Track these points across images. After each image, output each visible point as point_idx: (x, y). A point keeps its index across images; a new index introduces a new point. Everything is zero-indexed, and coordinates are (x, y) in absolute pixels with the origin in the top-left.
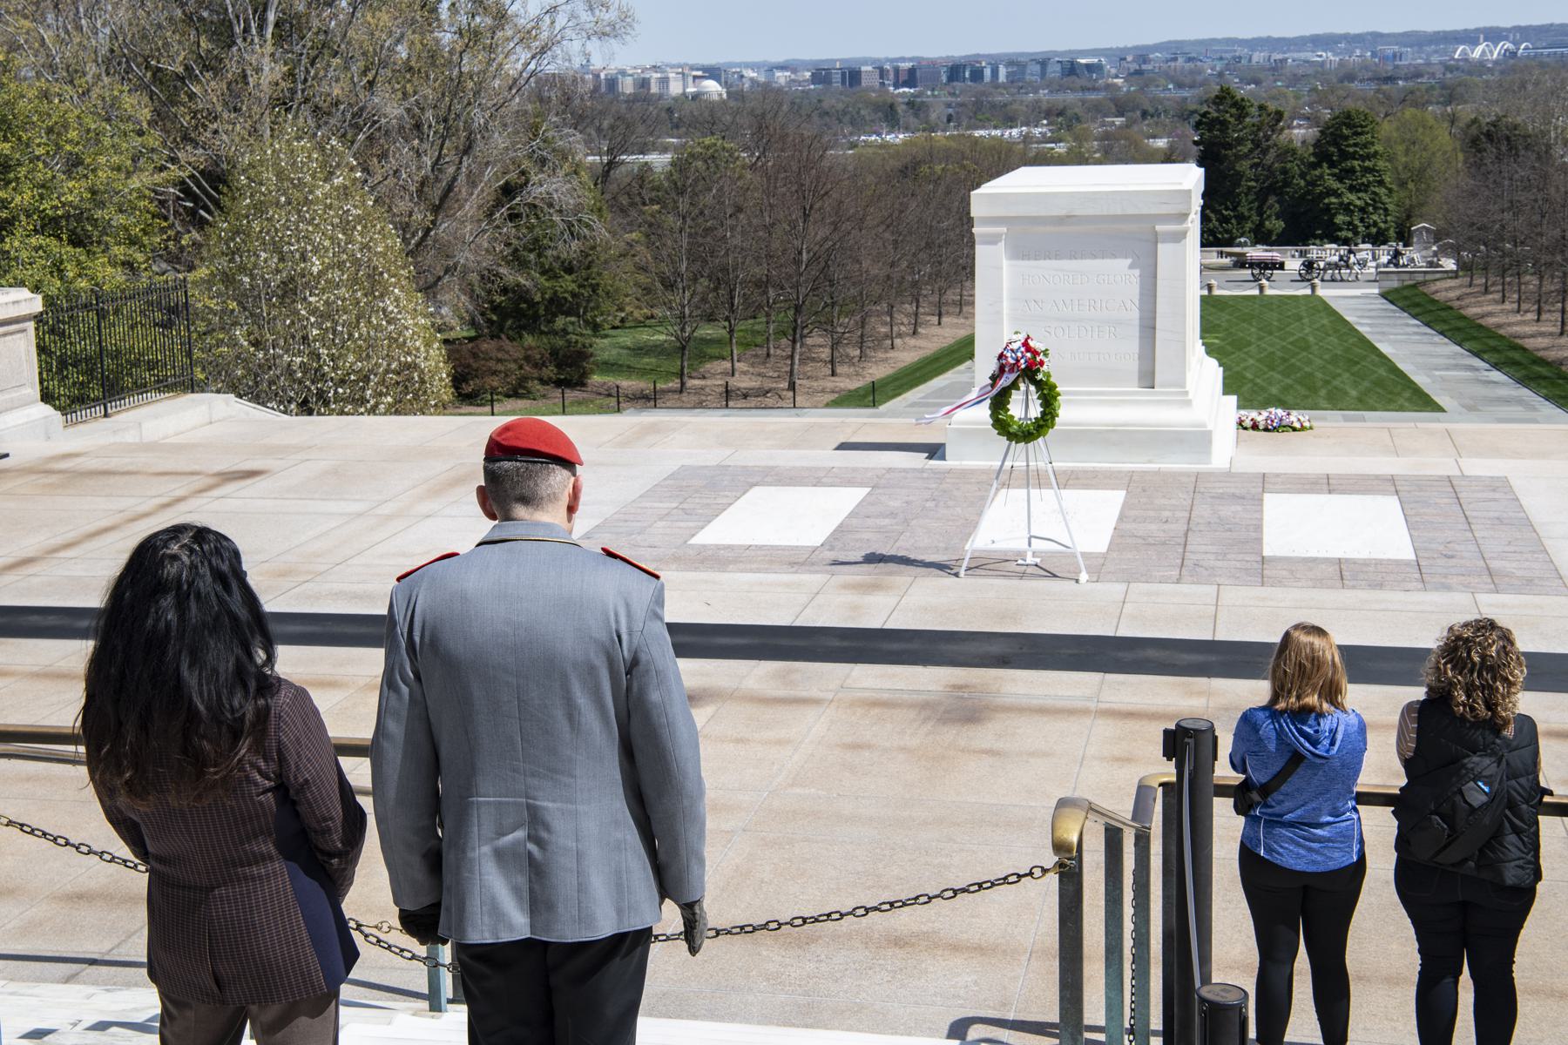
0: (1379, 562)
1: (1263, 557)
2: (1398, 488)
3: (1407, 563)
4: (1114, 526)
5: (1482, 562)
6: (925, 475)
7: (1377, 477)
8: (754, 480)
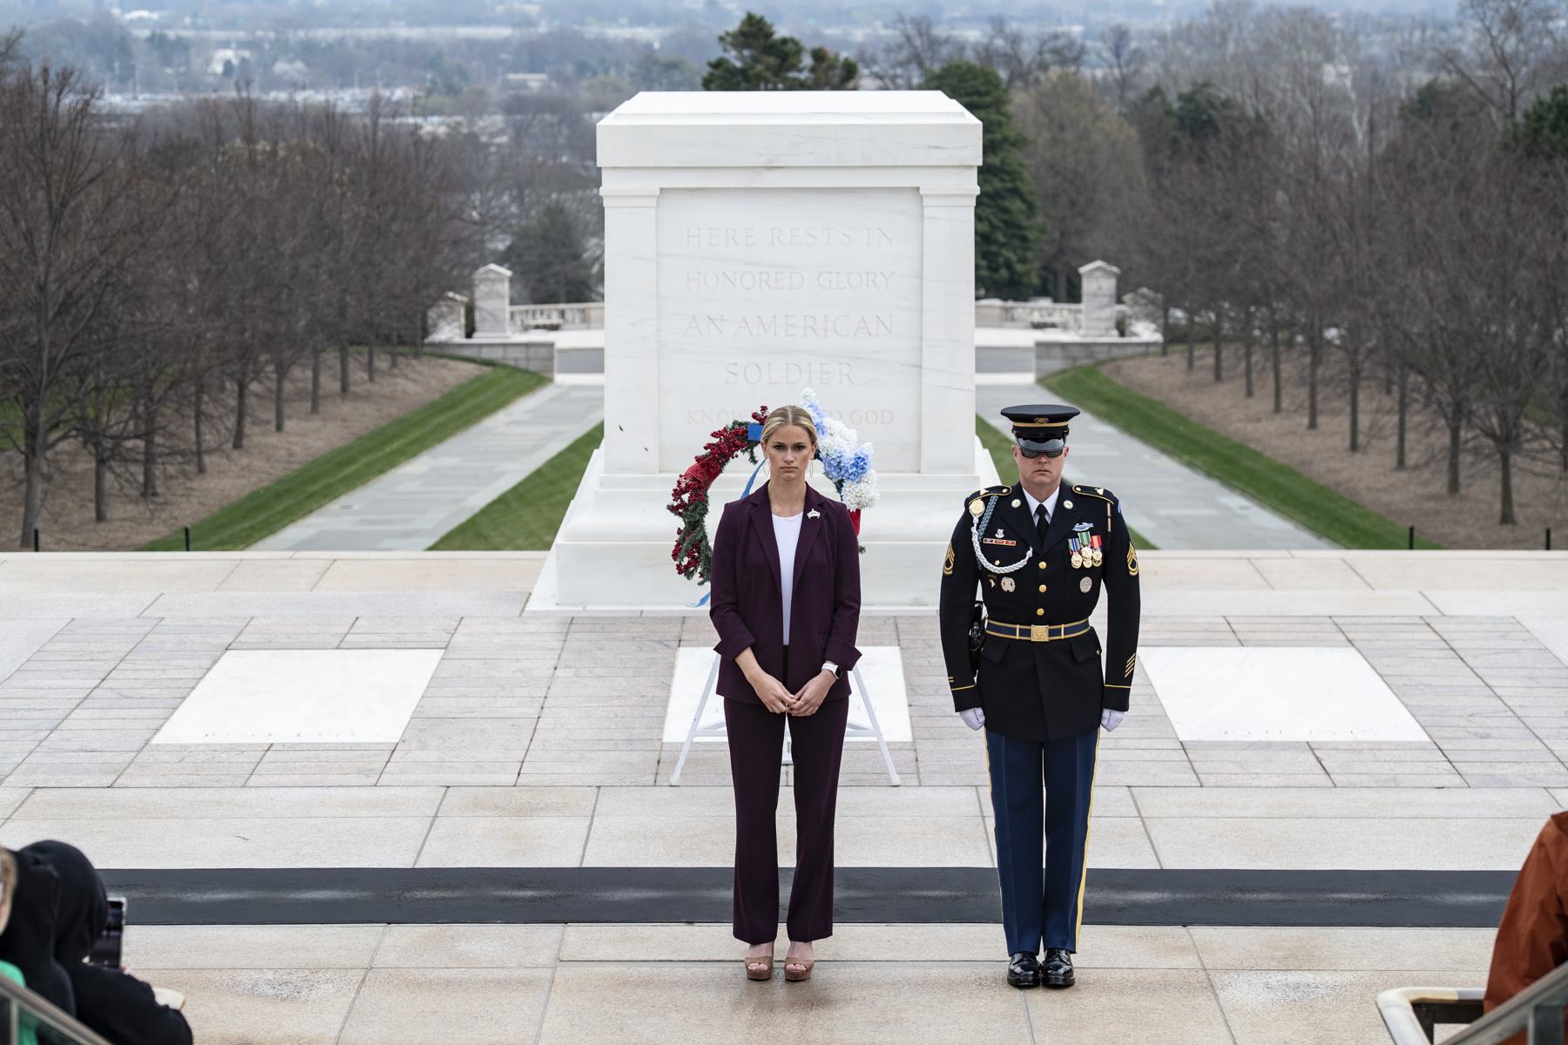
0: (1376, 747)
1: (1181, 742)
2: (1350, 636)
3: (1421, 748)
4: (906, 704)
5: (1538, 742)
6: (532, 628)
7: (1306, 619)
8: (228, 639)
